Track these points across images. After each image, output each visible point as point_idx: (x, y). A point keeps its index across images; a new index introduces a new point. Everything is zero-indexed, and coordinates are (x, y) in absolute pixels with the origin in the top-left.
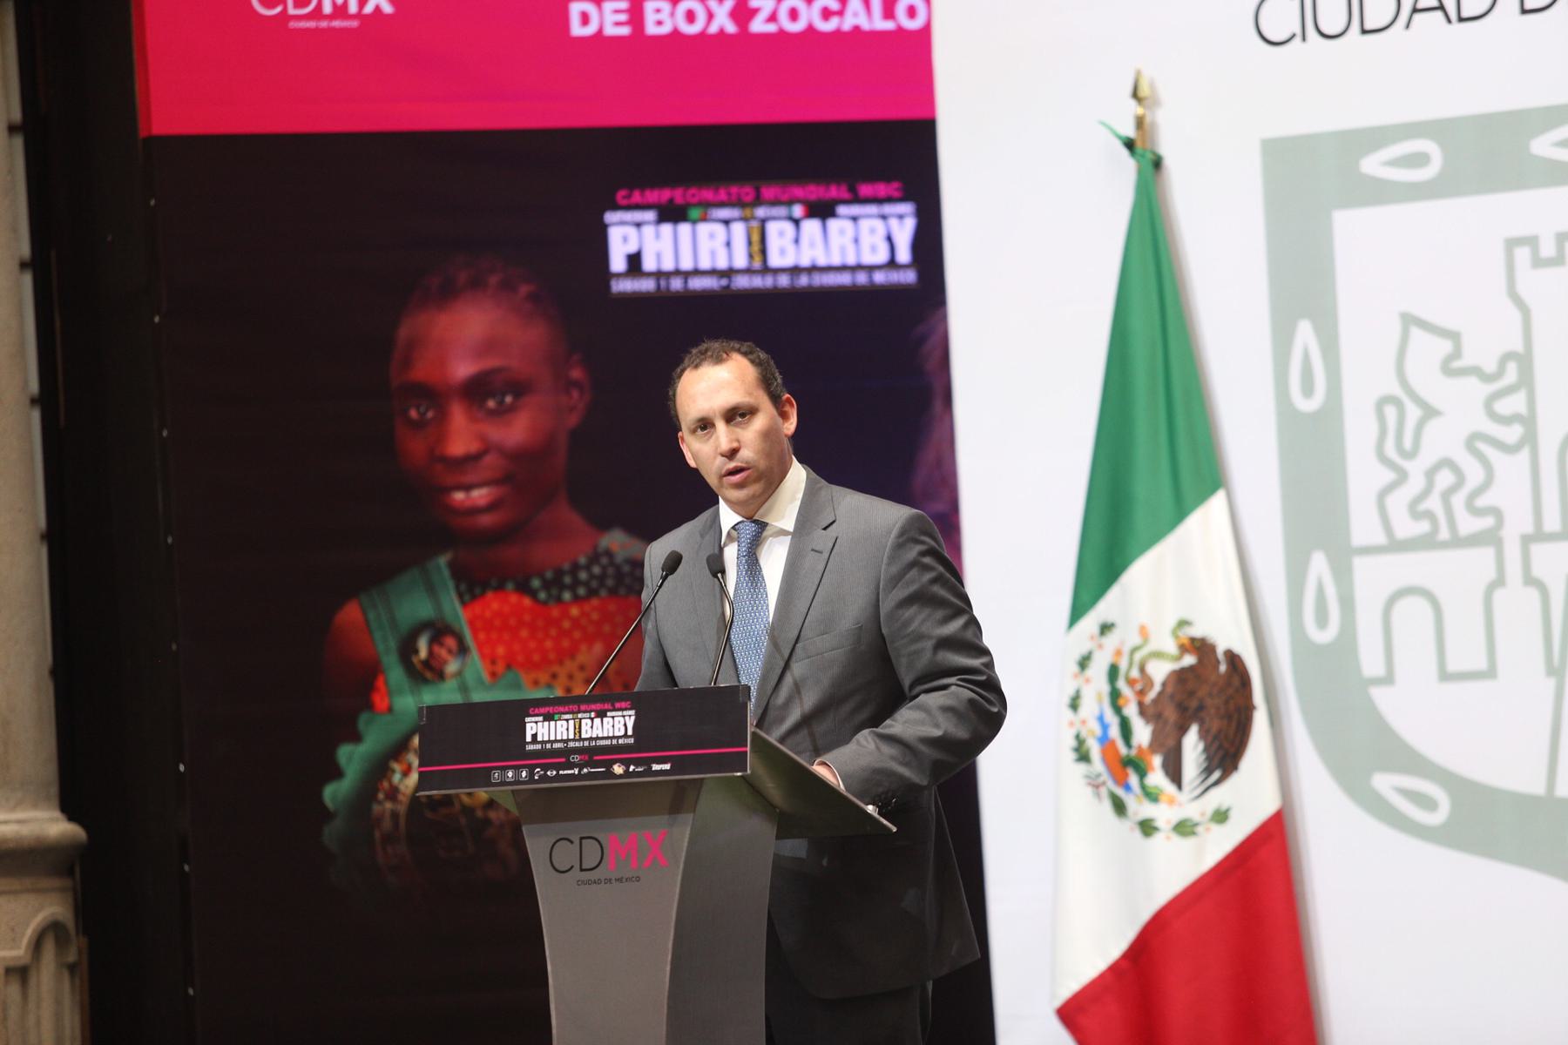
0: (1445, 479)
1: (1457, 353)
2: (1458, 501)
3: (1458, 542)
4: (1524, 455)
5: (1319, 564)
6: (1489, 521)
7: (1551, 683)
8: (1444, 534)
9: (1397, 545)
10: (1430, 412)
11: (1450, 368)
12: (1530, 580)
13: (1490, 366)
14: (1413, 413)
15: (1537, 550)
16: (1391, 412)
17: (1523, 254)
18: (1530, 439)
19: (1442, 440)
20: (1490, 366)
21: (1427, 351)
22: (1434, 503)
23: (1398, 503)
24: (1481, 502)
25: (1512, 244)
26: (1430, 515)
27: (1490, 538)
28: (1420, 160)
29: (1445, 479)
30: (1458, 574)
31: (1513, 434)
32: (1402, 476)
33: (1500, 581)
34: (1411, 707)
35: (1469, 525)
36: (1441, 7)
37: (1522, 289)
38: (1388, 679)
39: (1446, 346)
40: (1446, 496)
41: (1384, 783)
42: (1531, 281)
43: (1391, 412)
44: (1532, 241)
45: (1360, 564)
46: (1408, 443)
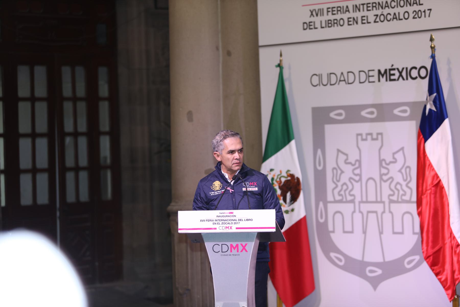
0: (345, 187)
1: (347, 159)
2: (347, 192)
3: (347, 202)
4: (359, 183)
5: (321, 205)
6: (352, 198)
7: (363, 235)
8: (344, 200)
9: (335, 202)
10: (342, 172)
11: (346, 162)
12: (360, 212)
14: (339, 172)
15: (362, 205)
16: (335, 171)
17: (360, 137)
18: (360, 180)
19: (344, 178)
20: (353, 163)
21: (342, 158)
22: (342, 193)
23: (336, 191)
24: (352, 193)
25: (358, 135)
26: (341, 195)
27: (352, 201)
28: (340, 115)
29: (345, 187)
30: (347, 208)
31: (357, 178)
32: (337, 186)
33: (354, 212)
34: (338, 238)
35: (349, 198)
36: (345, 80)
37: (359, 145)
38: (333, 232)
39: (345, 157)
40: (345, 191)
41: (333, 255)
42: (361, 143)
43: (335, 171)
44: (361, 135)
45: (329, 205)
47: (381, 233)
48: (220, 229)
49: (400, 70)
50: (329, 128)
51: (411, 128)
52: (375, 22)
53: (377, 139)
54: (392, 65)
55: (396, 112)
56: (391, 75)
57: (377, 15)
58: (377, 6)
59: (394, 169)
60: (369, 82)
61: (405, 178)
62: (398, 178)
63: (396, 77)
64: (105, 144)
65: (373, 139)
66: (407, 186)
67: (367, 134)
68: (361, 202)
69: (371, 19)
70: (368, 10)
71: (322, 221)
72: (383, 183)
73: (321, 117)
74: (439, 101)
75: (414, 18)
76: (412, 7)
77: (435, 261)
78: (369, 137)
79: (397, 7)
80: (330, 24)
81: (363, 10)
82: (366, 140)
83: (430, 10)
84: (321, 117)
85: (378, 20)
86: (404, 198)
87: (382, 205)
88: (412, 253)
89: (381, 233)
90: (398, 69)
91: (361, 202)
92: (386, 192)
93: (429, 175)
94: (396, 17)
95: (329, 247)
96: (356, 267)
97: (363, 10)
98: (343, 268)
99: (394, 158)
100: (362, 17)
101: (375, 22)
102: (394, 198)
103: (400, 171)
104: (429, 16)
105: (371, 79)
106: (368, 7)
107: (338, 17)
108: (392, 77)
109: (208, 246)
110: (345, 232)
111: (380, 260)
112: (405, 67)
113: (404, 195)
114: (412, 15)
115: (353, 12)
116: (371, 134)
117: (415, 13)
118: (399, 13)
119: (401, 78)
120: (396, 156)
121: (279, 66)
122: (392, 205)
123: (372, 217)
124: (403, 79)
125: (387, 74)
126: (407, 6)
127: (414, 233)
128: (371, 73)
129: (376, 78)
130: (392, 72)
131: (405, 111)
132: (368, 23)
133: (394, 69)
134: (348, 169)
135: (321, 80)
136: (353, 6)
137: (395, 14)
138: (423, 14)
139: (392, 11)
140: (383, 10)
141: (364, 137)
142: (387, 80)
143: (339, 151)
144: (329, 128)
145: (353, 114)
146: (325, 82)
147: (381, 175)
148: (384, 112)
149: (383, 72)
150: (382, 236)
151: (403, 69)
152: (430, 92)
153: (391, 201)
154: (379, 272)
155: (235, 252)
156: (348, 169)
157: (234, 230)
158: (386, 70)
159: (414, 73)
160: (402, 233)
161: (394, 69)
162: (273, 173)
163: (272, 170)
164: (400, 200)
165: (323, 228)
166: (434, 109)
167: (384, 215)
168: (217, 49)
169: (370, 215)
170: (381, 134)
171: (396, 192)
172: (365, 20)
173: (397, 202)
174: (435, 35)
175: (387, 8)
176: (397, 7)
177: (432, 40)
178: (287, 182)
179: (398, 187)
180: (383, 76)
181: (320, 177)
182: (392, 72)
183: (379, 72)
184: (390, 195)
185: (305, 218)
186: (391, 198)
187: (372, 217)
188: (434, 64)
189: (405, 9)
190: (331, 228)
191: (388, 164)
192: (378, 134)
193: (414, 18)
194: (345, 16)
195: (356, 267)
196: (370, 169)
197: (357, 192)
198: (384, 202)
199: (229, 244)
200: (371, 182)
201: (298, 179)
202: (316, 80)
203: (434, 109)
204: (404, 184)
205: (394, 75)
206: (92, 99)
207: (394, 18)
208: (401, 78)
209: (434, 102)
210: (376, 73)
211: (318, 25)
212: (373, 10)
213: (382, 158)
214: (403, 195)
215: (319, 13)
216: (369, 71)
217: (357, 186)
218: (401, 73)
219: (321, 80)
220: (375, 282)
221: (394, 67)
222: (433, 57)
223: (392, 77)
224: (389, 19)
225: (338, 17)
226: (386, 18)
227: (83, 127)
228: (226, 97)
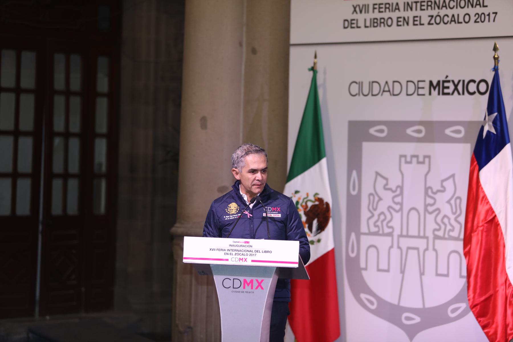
0: (382, 217)
1: (387, 184)
2: (385, 223)
3: (384, 235)
4: (399, 214)
5: (353, 236)
6: (390, 230)
7: (401, 275)
8: (381, 232)
9: (370, 234)
10: (380, 199)
11: (386, 188)
12: (399, 247)
13: (394, 189)
14: (377, 199)
15: (402, 240)
16: (372, 197)
17: (403, 159)
18: (401, 209)
19: (382, 207)
20: (394, 189)
21: (381, 182)
22: (379, 223)
23: (372, 222)
24: (390, 224)
25: (401, 156)
27: (390, 234)
28: (382, 131)
29: (382, 217)
31: (397, 207)
32: (373, 216)
33: (391, 247)
34: (371, 277)
35: (387, 230)
36: (389, 91)
38: (366, 269)
39: (384, 182)
41: (363, 296)
42: (404, 166)
43: (372, 197)
44: (405, 156)
45: (363, 238)
46: (375, 207)
47: (422, 274)
48: (233, 261)
49: (456, 82)
50: (367, 147)
51: (465, 152)
52: (429, 24)
53: (423, 163)
54: (447, 77)
55: (448, 132)
56: (444, 88)
57: (432, 16)
58: (433, 6)
59: (442, 199)
60: (418, 95)
61: (454, 210)
62: (446, 210)
63: (450, 91)
64: (101, 147)
65: (419, 163)
66: (456, 220)
67: (413, 156)
68: (401, 236)
69: (425, 20)
70: (421, 10)
71: (353, 255)
72: (428, 215)
73: (359, 132)
74: (501, 123)
75: (476, 22)
76: (474, 9)
77: (483, 311)
78: (414, 160)
79: (457, 8)
80: (375, 23)
81: (416, 9)
82: (410, 162)
83: (496, 13)
84: (359, 132)
85: (433, 21)
86: (452, 234)
87: (425, 241)
88: (456, 300)
89: (422, 274)
90: (453, 81)
91: (401, 236)
92: (431, 225)
93: (482, 209)
94: (454, 20)
95: (360, 287)
96: (390, 312)
97: (416, 9)
98: (374, 312)
99: (442, 186)
100: (414, 17)
101: (429, 24)
102: (440, 233)
103: (449, 202)
104: (494, 21)
105: (421, 91)
106: (421, 6)
107: (386, 15)
108: (446, 91)
109: (218, 279)
110: (379, 270)
111: (420, 306)
112: (462, 79)
113: (453, 230)
114: (473, 19)
115: (404, 10)
116: (417, 156)
117: (477, 16)
118: (458, 15)
119: (456, 92)
120: (445, 184)
121: (313, 69)
122: (437, 241)
123: (413, 254)
124: (459, 94)
125: (439, 87)
126: (468, 7)
127: (461, 277)
128: (421, 85)
129: (426, 91)
130: (446, 85)
131: (458, 132)
132: (421, 24)
133: (448, 81)
134: (387, 197)
135: (361, 89)
136: (405, 3)
137: (453, 16)
138: (487, 17)
139: (450, 12)
140: (440, 11)
141: (409, 159)
142: (439, 94)
143: (377, 174)
144: (367, 147)
145: (397, 131)
146: (366, 91)
147: (426, 206)
148: (434, 132)
149: (435, 83)
150: (423, 277)
151: (459, 81)
152: (490, 110)
153: (436, 237)
154: (417, 319)
155: (248, 288)
156: (387, 197)
157: (249, 263)
158: (439, 82)
159: (472, 87)
160: (447, 275)
161: (448, 81)
162: (298, 195)
163: (297, 192)
164: (446, 236)
165: (354, 264)
166: (493, 131)
167: (427, 252)
168: (241, 45)
169: (410, 251)
170: (429, 157)
171: (443, 227)
172: (417, 21)
173: (443, 238)
174: (500, 44)
175: (444, 8)
176: (457, 8)
177: (495, 49)
178: (313, 207)
179: (446, 220)
180: (435, 89)
181: (354, 203)
182: (446, 85)
183: (431, 83)
184: (435, 230)
185: (333, 251)
186: (437, 233)
187: (413, 254)
188: (496, 79)
189: (466, 10)
190: (363, 265)
191: (435, 193)
192: (425, 157)
193: (476, 22)
194: (394, 15)
195: (390, 312)
196: (414, 197)
197: (396, 223)
198: (427, 238)
199: (242, 279)
200: (413, 213)
201: (327, 204)
202: (355, 89)
203: (493, 131)
204: (452, 217)
205: (448, 88)
206: (89, 95)
207: (452, 21)
208: (456, 92)
209: (494, 123)
210: (427, 85)
211: (361, 23)
212: (427, 9)
213: (428, 185)
214: (450, 230)
215: (363, 9)
216: (419, 81)
217: (397, 216)
218: (456, 86)
219: (361, 89)
220: (412, 332)
221: (448, 79)
222: (496, 69)
223: (446, 91)
224: (446, 21)
225: (386, 15)
226: (442, 20)
227: (75, 127)
228: (248, 102)
